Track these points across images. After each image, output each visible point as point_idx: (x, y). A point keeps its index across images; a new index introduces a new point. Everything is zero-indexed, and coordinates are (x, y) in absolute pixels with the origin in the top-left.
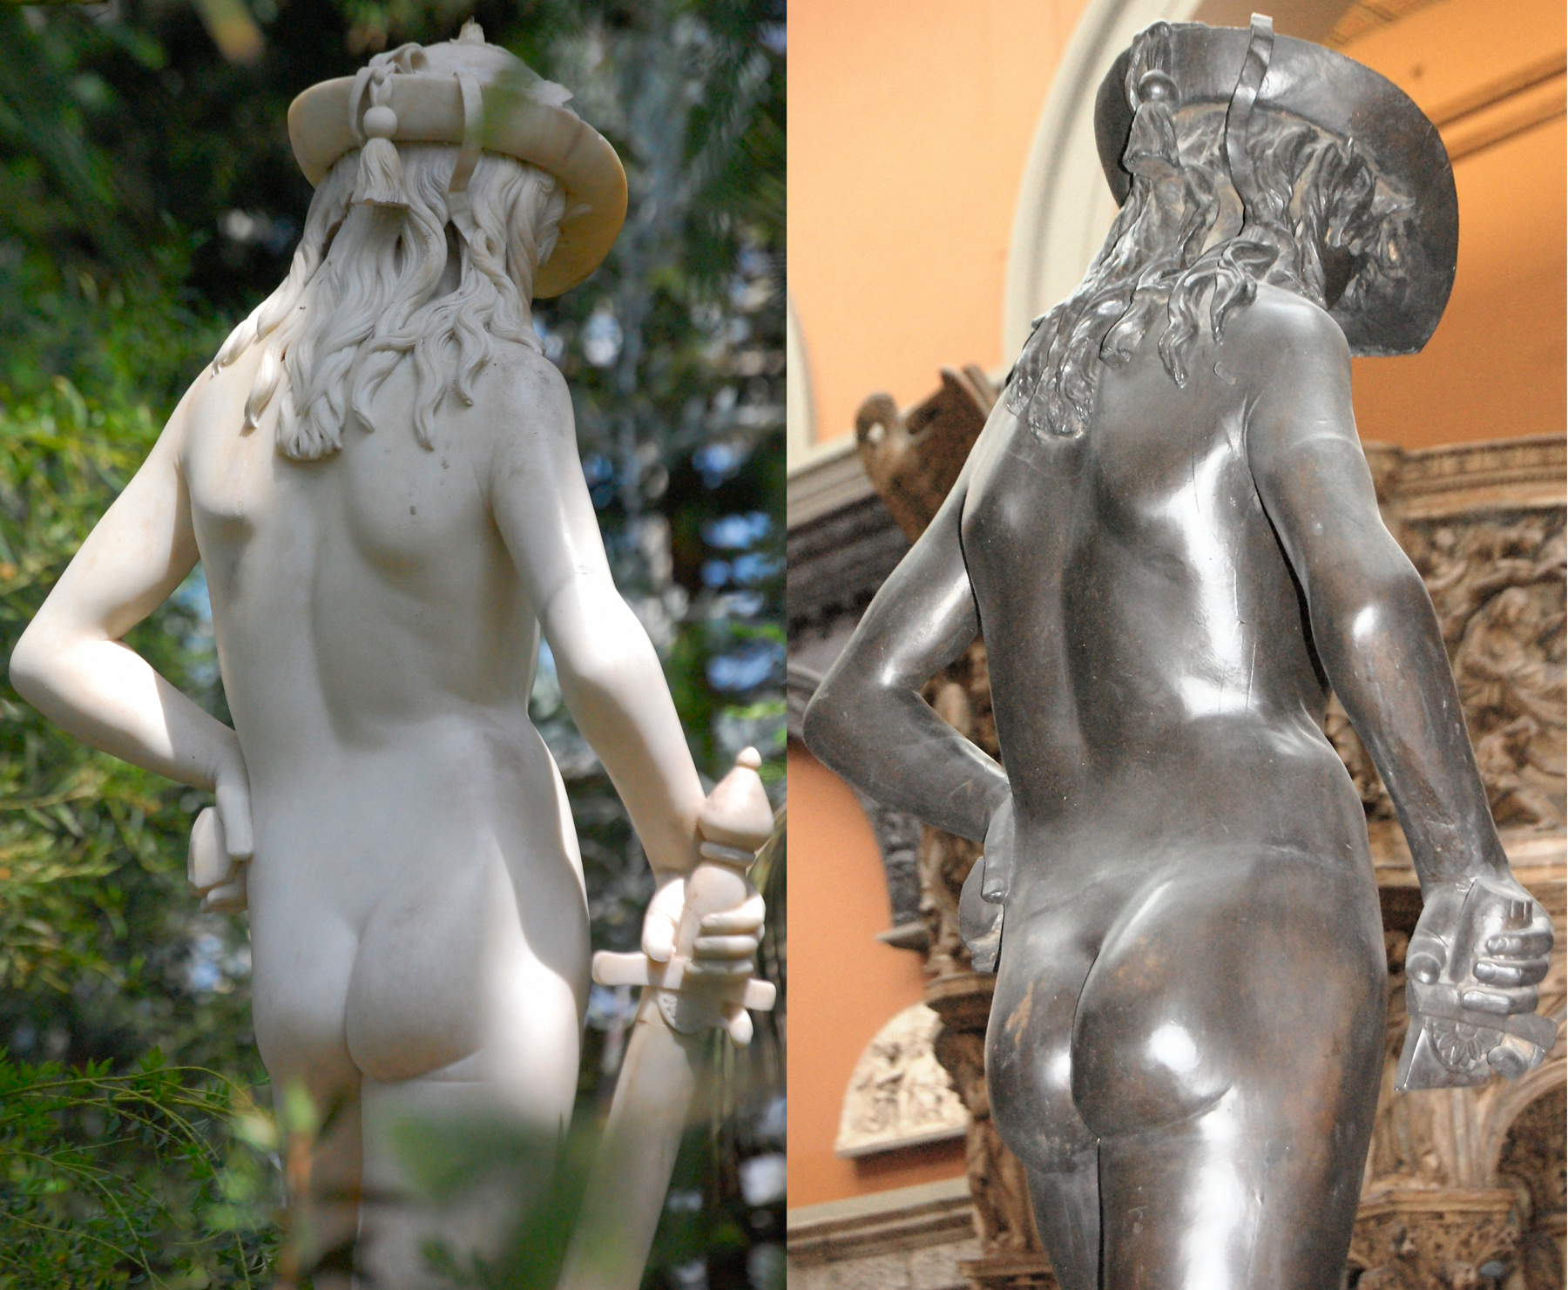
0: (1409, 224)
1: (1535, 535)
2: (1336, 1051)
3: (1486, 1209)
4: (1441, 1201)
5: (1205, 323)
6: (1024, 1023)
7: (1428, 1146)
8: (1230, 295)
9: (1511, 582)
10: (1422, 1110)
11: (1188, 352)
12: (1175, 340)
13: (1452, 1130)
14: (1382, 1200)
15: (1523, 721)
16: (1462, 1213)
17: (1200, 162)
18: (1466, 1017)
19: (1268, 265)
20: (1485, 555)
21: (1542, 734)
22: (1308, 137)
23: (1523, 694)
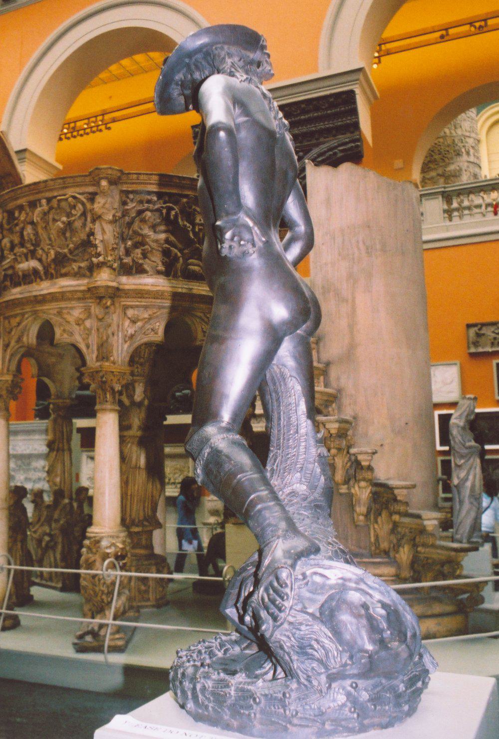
9: (147, 209)
13: (118, 351)
15: (147, 247)
16: (119, 372)
20: (141, 202)
23: (147, 240)
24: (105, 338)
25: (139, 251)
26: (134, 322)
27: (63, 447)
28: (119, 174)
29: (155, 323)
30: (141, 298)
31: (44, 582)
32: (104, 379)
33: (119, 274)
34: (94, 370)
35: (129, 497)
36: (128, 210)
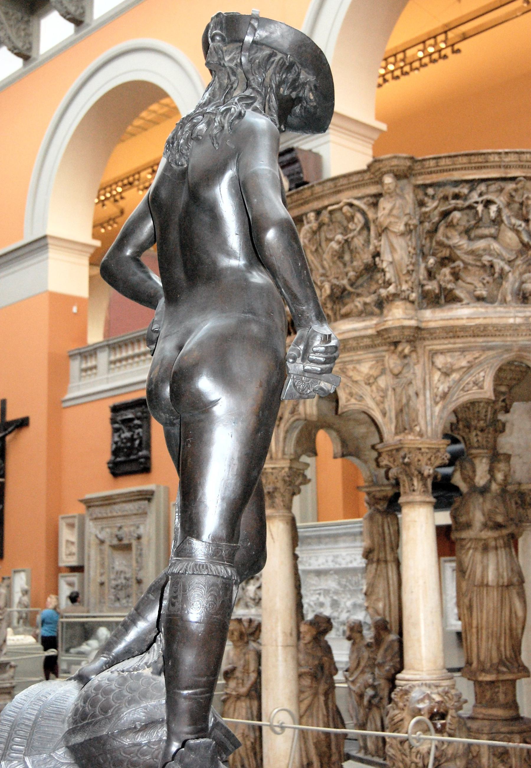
0: (315, 86)
1: (465, 191)
2: (261, 386)
3: (437, 446)
4: (421, 444)
5: (226, 125)
6: (156, 374)
7: (416, 423)
8: (235, 115)
9: (455, 209)
10: (414, 409)
11: (219, 137)
12: (215, 132)
14: (398, 443)
15: (458, 263)
16: (428, 448)
17: (232, 65)
18: (306, 375)
19: (252, 104)
20: (445, 198)
21: (465, 268)
22: (271, 56)
23: (458, 253)
24: (404, 401)
25: (446, 271)
26: (446, 374)
27: (386, 557)
28: (408, 163)
29: (479, 373)
30: (454, 337)
31: (369, 757)
32: (406, 460)
33: (421, 308)
34: (393, 447)
35: (474, 630)
36: (426, 213)
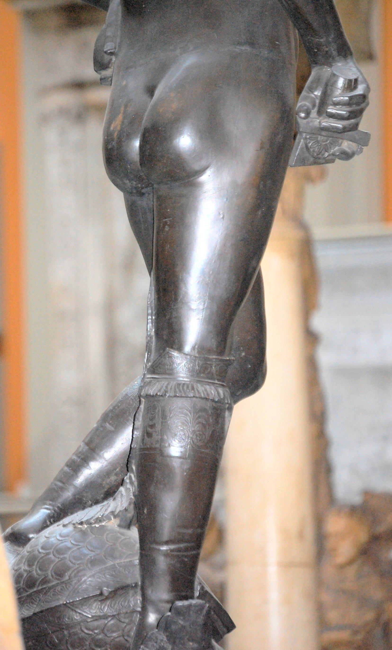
2: (262, 148)
18: (323, 133)
